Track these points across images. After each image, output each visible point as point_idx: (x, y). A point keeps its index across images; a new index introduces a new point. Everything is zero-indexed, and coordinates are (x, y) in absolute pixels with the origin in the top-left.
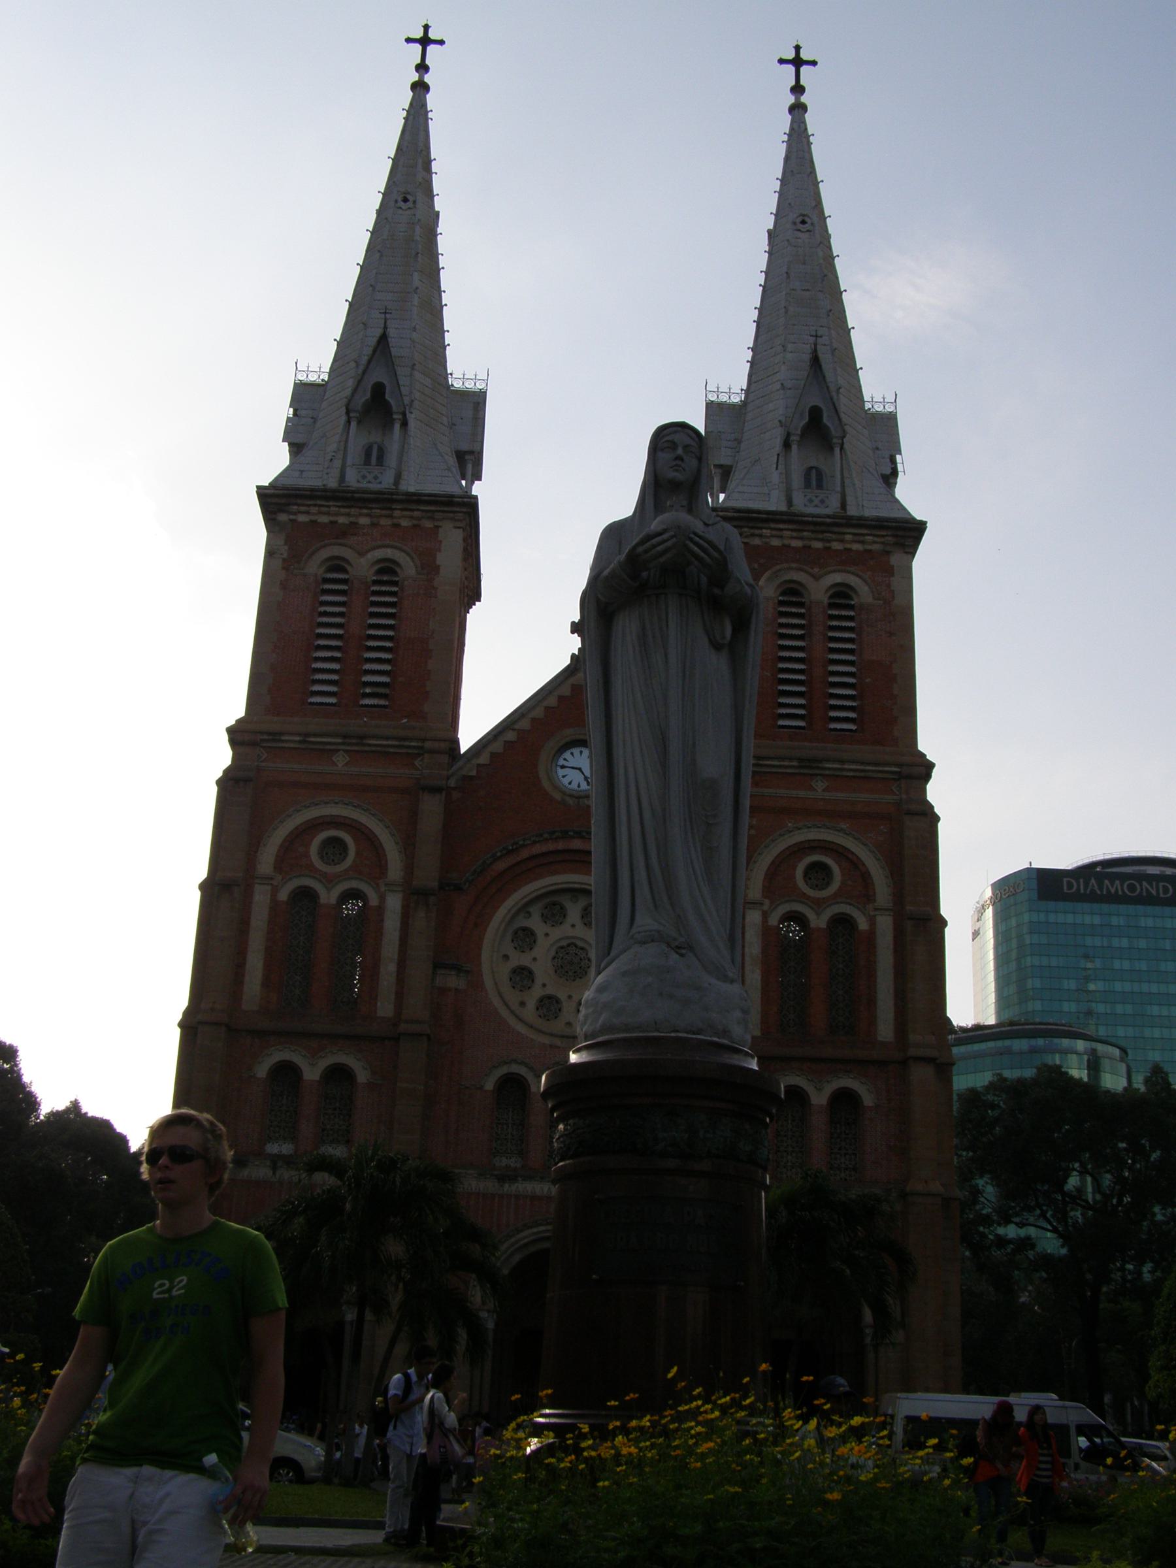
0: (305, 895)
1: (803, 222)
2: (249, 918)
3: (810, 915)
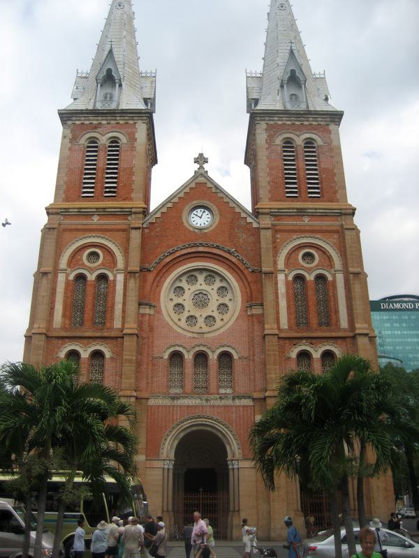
0: (81, 277)
1: (282, 7)
2: (56, 287)
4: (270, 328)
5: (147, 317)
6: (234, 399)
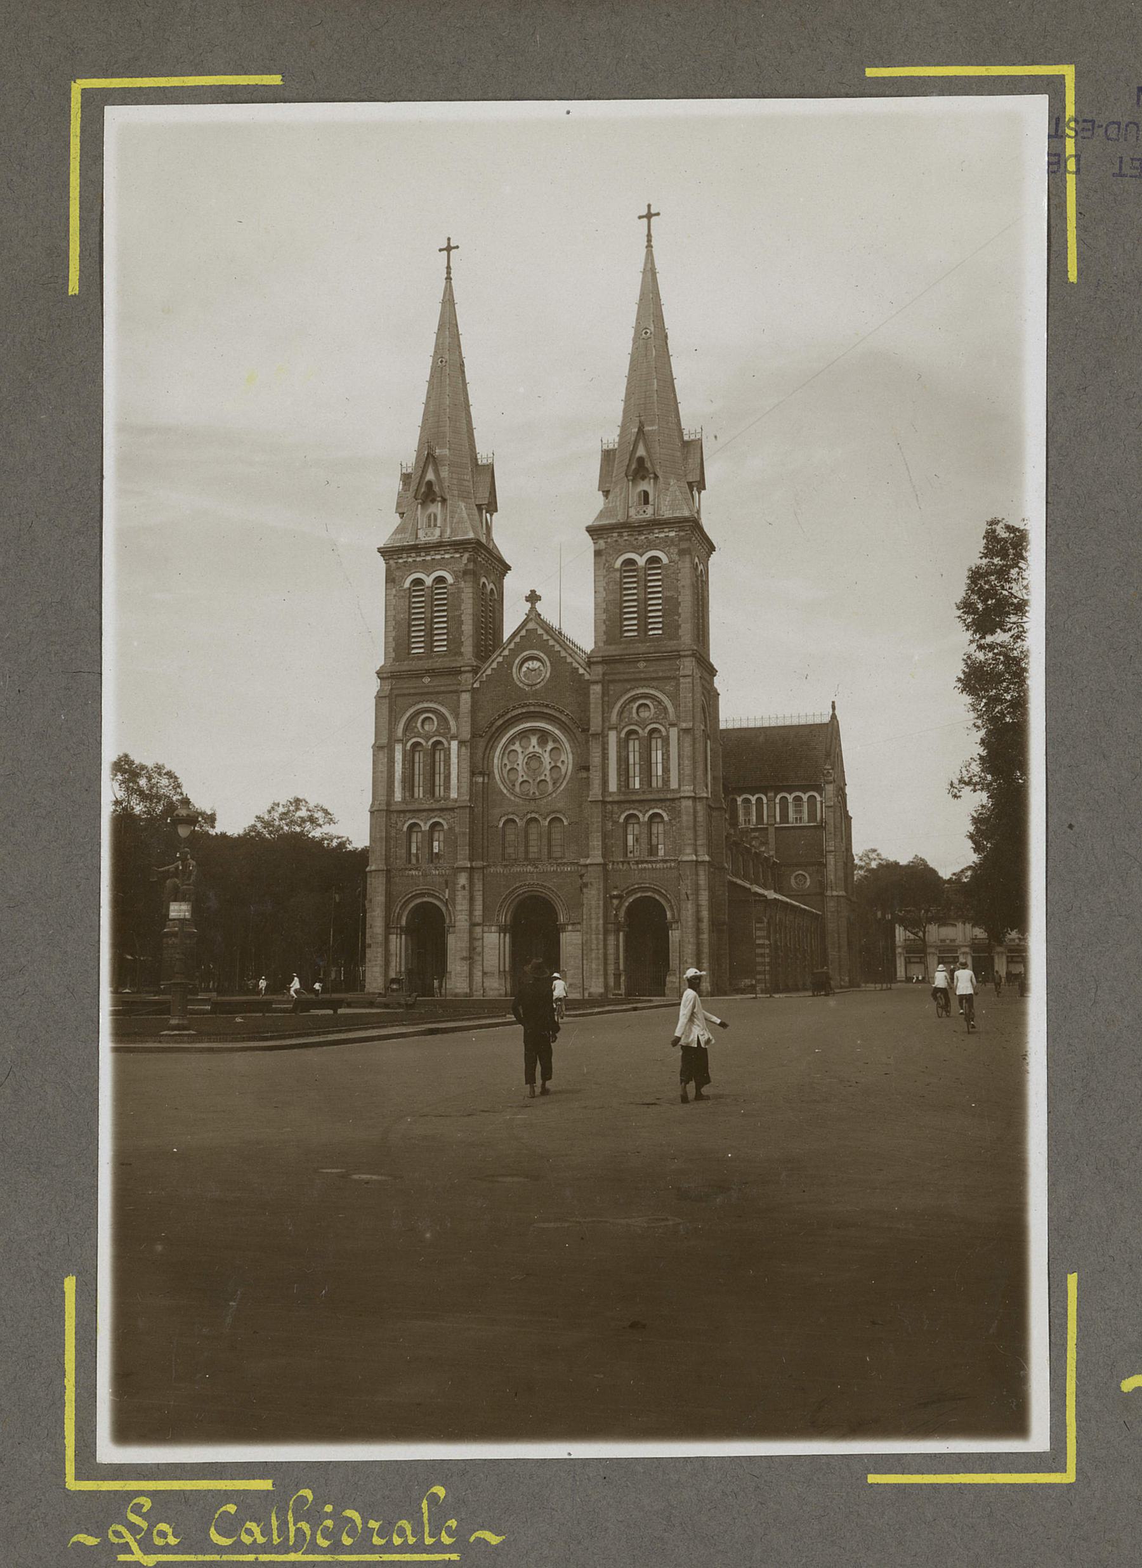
4: (595, 792)
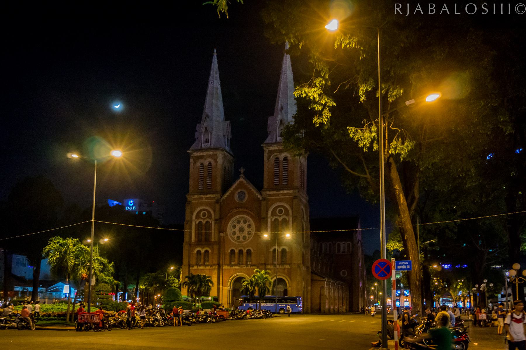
0: (200, 223)
3: (279, 218)
5: (223, 237)
6: (250, 267)
